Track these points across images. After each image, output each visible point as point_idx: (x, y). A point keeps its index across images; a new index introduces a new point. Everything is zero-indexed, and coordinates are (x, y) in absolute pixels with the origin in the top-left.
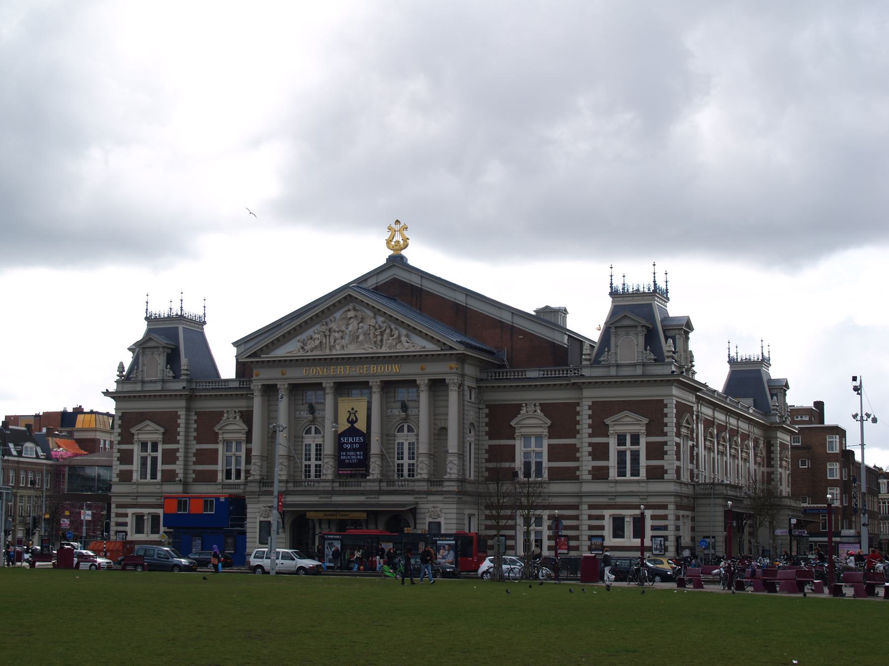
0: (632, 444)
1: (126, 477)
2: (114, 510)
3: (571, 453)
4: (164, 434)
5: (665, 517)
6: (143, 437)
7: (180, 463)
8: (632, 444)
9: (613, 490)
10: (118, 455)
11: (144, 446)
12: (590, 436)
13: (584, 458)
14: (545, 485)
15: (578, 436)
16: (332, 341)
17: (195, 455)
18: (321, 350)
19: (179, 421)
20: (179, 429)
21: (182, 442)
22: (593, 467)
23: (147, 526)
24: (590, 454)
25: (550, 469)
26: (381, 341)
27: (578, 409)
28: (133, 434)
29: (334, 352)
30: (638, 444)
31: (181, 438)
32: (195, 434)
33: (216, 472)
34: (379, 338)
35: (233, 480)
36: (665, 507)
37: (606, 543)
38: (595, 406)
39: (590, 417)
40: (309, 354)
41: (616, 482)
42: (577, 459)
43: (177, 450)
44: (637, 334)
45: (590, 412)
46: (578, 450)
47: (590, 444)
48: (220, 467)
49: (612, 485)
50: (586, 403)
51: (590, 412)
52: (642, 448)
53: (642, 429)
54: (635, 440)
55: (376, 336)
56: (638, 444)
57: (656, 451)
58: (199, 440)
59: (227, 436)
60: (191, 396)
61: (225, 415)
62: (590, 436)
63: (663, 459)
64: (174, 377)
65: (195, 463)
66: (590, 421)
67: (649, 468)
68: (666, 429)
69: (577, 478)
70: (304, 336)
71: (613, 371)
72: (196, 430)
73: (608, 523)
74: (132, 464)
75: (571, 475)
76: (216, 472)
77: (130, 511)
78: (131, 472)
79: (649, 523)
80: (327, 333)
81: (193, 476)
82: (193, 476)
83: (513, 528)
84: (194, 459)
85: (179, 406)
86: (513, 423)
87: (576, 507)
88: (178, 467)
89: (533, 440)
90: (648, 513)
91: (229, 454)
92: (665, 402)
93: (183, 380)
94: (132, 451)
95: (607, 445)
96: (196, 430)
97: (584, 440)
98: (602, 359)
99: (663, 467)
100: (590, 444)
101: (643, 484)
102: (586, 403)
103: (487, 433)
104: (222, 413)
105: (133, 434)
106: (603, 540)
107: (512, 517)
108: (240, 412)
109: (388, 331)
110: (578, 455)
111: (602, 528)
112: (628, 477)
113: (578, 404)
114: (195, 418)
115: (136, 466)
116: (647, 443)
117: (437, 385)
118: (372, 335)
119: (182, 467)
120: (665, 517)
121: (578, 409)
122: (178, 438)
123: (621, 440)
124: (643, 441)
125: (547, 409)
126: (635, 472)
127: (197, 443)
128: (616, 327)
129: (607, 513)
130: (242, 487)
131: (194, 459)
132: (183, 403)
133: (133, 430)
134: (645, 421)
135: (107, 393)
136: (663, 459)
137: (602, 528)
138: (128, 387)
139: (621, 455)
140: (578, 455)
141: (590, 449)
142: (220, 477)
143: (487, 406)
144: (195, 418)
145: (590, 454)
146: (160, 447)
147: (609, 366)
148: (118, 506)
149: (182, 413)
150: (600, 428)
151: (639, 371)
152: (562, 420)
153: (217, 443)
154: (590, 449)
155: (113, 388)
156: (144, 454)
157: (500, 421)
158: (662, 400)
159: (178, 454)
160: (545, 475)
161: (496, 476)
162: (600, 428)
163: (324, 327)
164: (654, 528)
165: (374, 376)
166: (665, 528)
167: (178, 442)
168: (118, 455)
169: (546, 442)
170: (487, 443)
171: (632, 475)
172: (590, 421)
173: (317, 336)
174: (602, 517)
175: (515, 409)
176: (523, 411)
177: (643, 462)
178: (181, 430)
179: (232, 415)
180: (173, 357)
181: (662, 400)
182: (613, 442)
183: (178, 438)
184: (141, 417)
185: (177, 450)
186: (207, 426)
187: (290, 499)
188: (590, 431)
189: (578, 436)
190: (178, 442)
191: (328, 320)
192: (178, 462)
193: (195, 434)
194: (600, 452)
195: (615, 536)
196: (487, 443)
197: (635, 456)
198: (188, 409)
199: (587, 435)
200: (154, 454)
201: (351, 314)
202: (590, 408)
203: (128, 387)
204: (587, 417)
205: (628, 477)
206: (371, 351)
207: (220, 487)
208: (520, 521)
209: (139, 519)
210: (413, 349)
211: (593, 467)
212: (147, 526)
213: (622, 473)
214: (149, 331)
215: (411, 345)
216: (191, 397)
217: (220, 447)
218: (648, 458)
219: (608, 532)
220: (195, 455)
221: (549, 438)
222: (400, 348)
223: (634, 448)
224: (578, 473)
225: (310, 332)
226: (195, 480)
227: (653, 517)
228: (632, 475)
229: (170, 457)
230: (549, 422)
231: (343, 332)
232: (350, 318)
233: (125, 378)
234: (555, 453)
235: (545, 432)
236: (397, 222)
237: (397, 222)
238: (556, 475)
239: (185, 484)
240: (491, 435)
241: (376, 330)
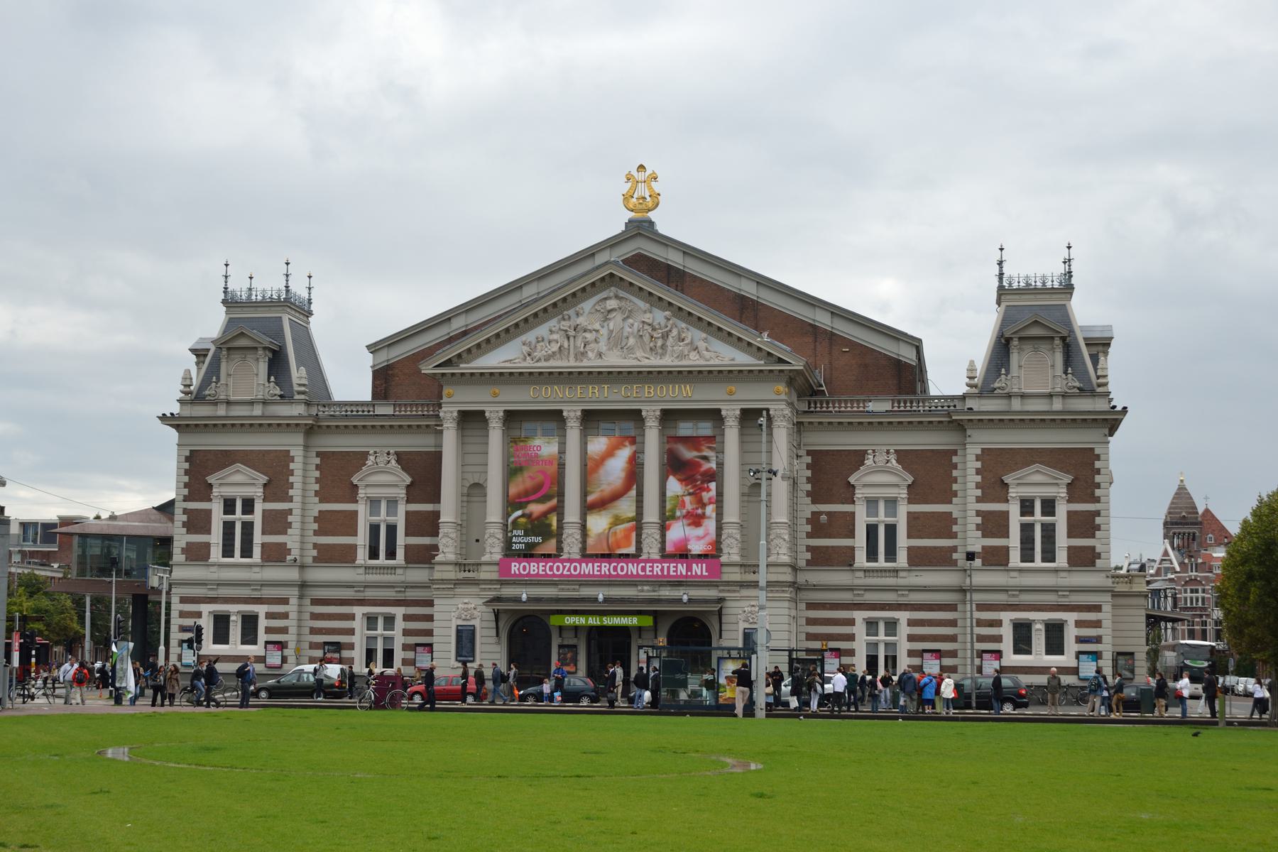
0: (1044, 514)
1: (198, 554)
2: (176, 607)
3: (944, 525)
4: (265, 485)
5: (1097, 624)
6: (229, 492)
7: (294, 531)
8: (1044, 514)
10: (185, 518)
11: (229, 506)
12: (979, 500)
13: (969, 534)
14: (901, 574)
15: (954, 500)
17: (316, 520)
19: (292, 466)
20: (291, 479)
21: (297, 499)
23: (235, 631)
24: (978, 527)
25: (909, 549)
27: (955, 459)
28: (211, 486)
30: (1053, 514)
31: (295, 493)
32: (317, 487)
33: (354, 548)
35: (382, 560)
37: (1005, 662)
38: (986, 455)
39: (978, 472)
41: (1021, 570)
42: (953, 536)
43: (290, 511)
44: (1053, 350)
45: (979, 464)
46: (955, 521)
47: (978, 513)
48: (361, 539)
50: (973, 450)
51: (979, 464)
52: (1060, 520)
53: (1062, 492)
54: (1049, 506)
56: (1053, 514)
58: (323, 496)
59: (374, 492)
60: (312, 427)
61: (372, 458)
62: (979, 500)
63: (1093, 536)
64: (281, 396)
65: (316, 533)
66: (979, 478)
67: (1071, 550)
68: (1098, 492)
69: (955, 563)
71: (1016, 404)
72: (318, 481)
73: (1007, 632)
74: (209, 532)
75: (942, 559)
76: (354, 548)
77: (206, 609)
78: (207, 546)
79: (1071, 633)
81: (315, 553)
82: (315, 553)
83: (851, 637)
84: (316, 526)
85: (293, 444)
86: (852, 480)
87: (952, 607)
88: (291, 540)
89: (882, 506)
90: (1070, 617)
91: (375, 519)
92: (1097, 452)
93: (299, 402)
94: (209, 512)
95: (1005, 515)
96: (318, 481)
97: (967, 505)
99: (1094, 548)
100: (978, 513)
102: (973, 450)
103: (809, 494)
104: (365, 455)
105: (211, 486)
106: (1001, 657)
107: (851, 622)
108: (397, 453)
110: (955, 528)
111: (998, 639)
112: (1038, 563)
113: (955, 452)
114: (318, 461)
115: (216, 537)
116: (1069, 512)
117: (749, 416)
119: (298, 538)
120: (1097, 624)
121: (955, 459)
122: (291, 492)
123: (1027, 507)
124: (1062, 509)
125: (904, 457)
126: (1049, 555)
127: (321, 501)
128: (1020, 339)
129: (1007, 617)
130: (399, 571)
131: (316, 526)
132: (299, 439)
133: (211, 479)
134: (1068, 479)
135: (163, 418)
136: (1093, 536)
137: (998, 639)
138: (202, 411)
139: (1027, 529)
140: (955, 528)
141: (979, 520)
142: (362, 556)
143: (809, 453)
144: (318, 461)
145: (978, 527)
146: (259, 507)
147: (1009, 396)
148: (184, 600)
149: (297, 452)
150: (994, 488)
151: (1057, 405)
152: (930, 475)
153: (357, 502)
154: (979, 520)
155: (176, 409)
156: (230, 517)
157: (829, 476)
158: (1092, 449)
159: (290, 519)
160: (902, 559)
161: (821, 558)
162: (994, 488)
164: (1080, 640)
166: (1098, 640)
167: (290, 500)
168: (185, 518)
169: (903, 510)
170: (807, 508)
171: (1044, 560)
172: (979, 478)
174: (998, 623)
175: (857, 458)
176: (869, 461)
177: (1062, 541)
178: (296, 479)
179: (382, 459)
180: (277, 362)
181: (1092, 449)
182: (1014, 509)
183: (291, 492)
184: (225, 459)
185: (290, 511)
186: (339, 476)
187: (508, 591)
188: (979, 492)
189: (954, 500)
190: (290, 500)
192: (289, 531)
193: (317, 487)
194: (994, 524)
195: (1017, 651)
196: (807, 508)
197: (1049, 531)
198: (306, 447)
199: (974, 499)
200: (247, 517)
202: (978, 458)
203: (202, 411)
204: (974, 471)
205: (1038, 563)
207: (362, 571)
208: (859, 630)
209: (221, 623)
211: (983, 547)
212: (235, 631)
213: (1027, 555)
214: (231, 323)
216: (311, 430)
217: (362, 509)
218: (1070, 535)
219: (1007, 645)
220: (316, 520)
221: (910, 502)
223: (1048, 519)
224: (955, 556)
226: (315, 559)
227: (1079, 624)
228: (1044, 560)
229: (277, 522)
230: (910, 480)
233: (194, 397)
234: (918, 525)
235: (903, 493)
238: (919, 558)
239: (302, 567)
240: (816, 497)
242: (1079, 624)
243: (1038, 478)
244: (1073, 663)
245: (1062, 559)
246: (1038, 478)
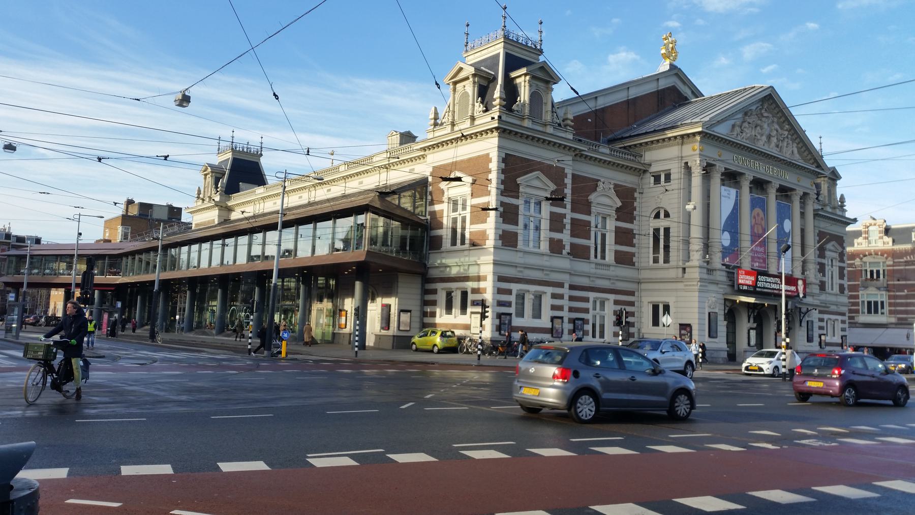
9: (522, 261)
22: (503, 231)
36: (560, 285)
41: (525, 252)
49: (520, 254)
57: (556, 223)
73: (512, 298)
79: (547, 302)
90: (549, 290)
95: (517, 207)
98: (514, 107)
101: (546, 258)
123: (527, 202)
129: (515, 287)
134: (552, 187)
150: (509, 187)
174: (509, 292)
227: (554, 296)
242: (554, 296)
243: (536, 183)
244: (549, 325)
245: (544, 247)
246: (536, 183)
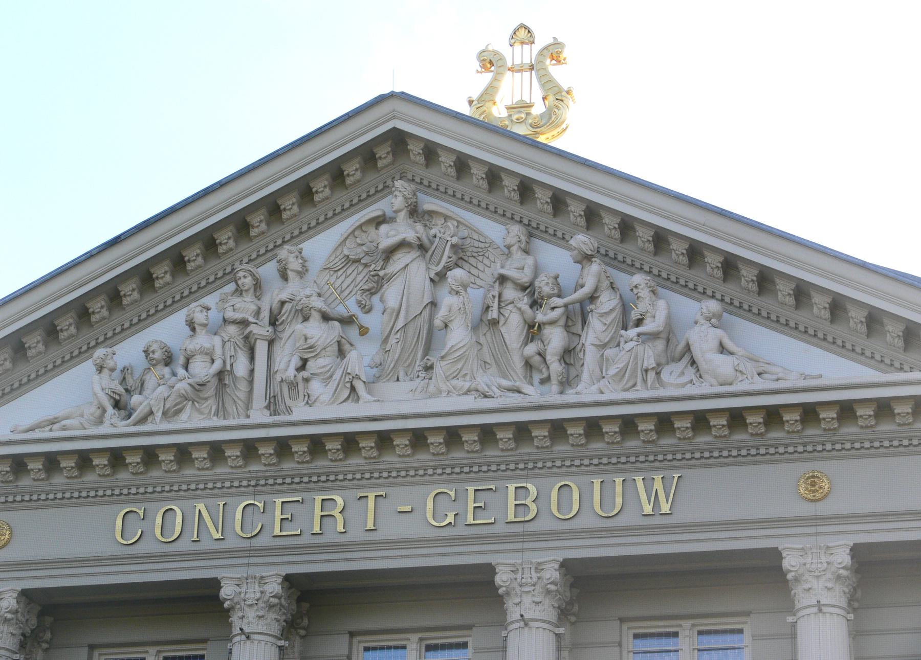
16: (286, 362)
18: (221, 411)
26: (568, 355)
29: (300, 412)
34: (556, 339)
40: (158, 424)
55: (533, 331)
70: (129, 352)
80: (261, 330)
109: (607, 302)
118: (513, 328)
163: (245, 306)
165: (522, 535)
173: (203, 340)
191: (268, 270)
201: (404, 229)
206: (514, 400)
210: (760, 384)
215: (749, 368)
222: (677, 388)
225: (168, 331)
231: (348, 321)
232: (390, 252)
236: (523, 34)
237: (523, 34)
241: (535, 304)
